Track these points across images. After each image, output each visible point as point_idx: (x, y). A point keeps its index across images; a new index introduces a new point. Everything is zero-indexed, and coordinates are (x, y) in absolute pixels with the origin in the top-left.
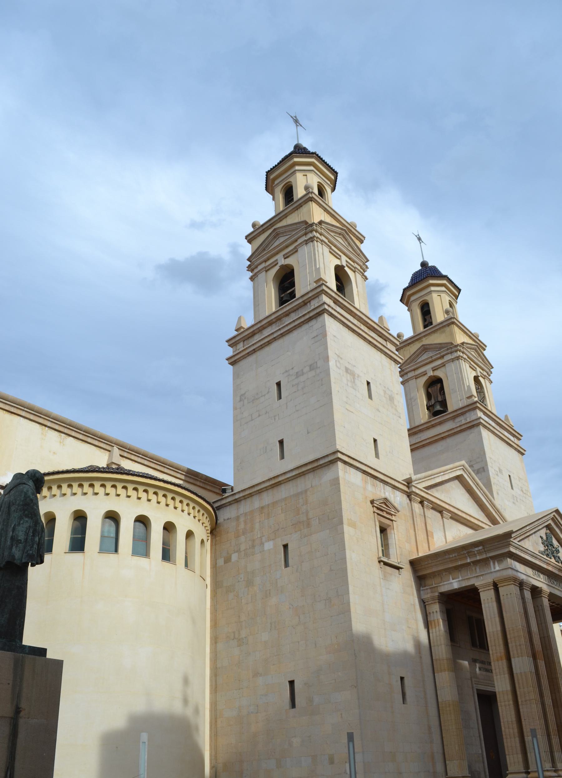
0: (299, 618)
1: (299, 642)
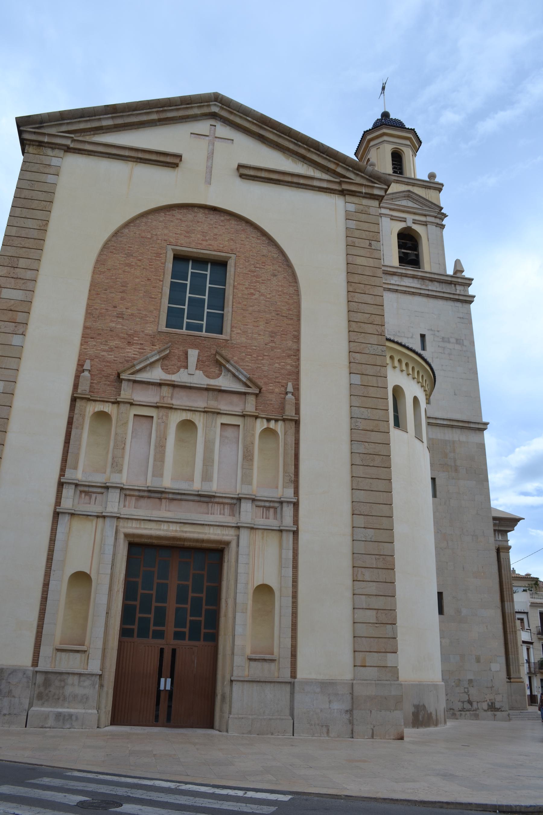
0: (447, 543)
1: (447, 563)
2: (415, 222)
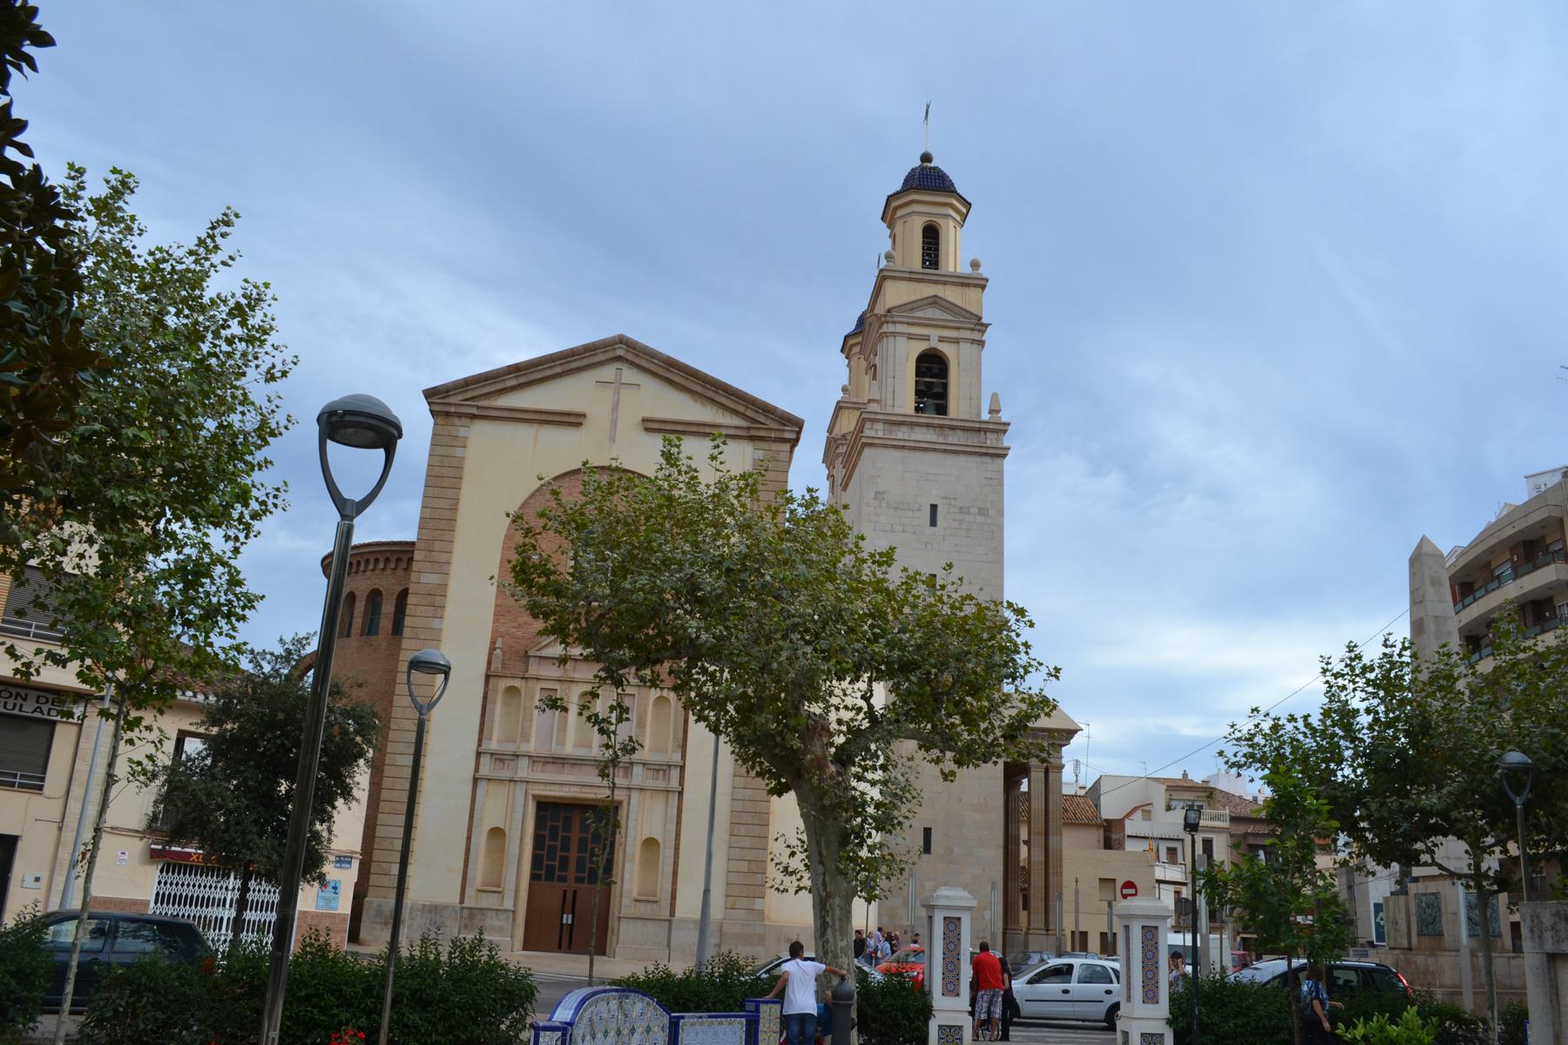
2: (941, 340)
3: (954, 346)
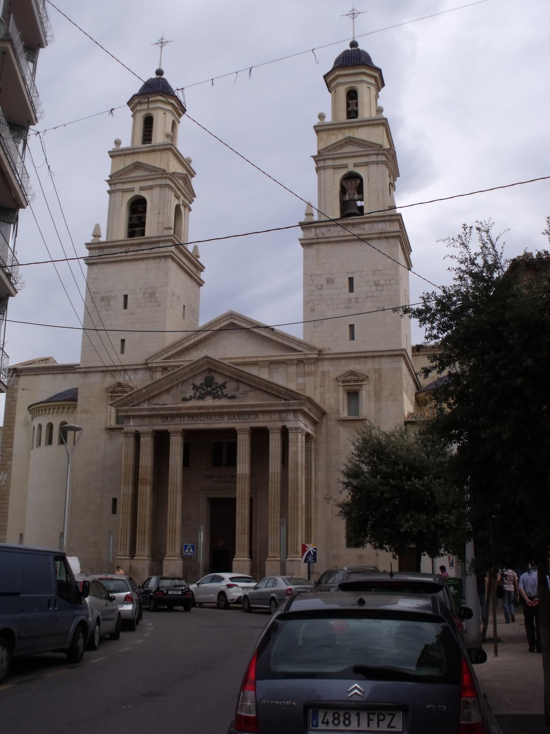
2: (356, 165)
3: (365, 168)
